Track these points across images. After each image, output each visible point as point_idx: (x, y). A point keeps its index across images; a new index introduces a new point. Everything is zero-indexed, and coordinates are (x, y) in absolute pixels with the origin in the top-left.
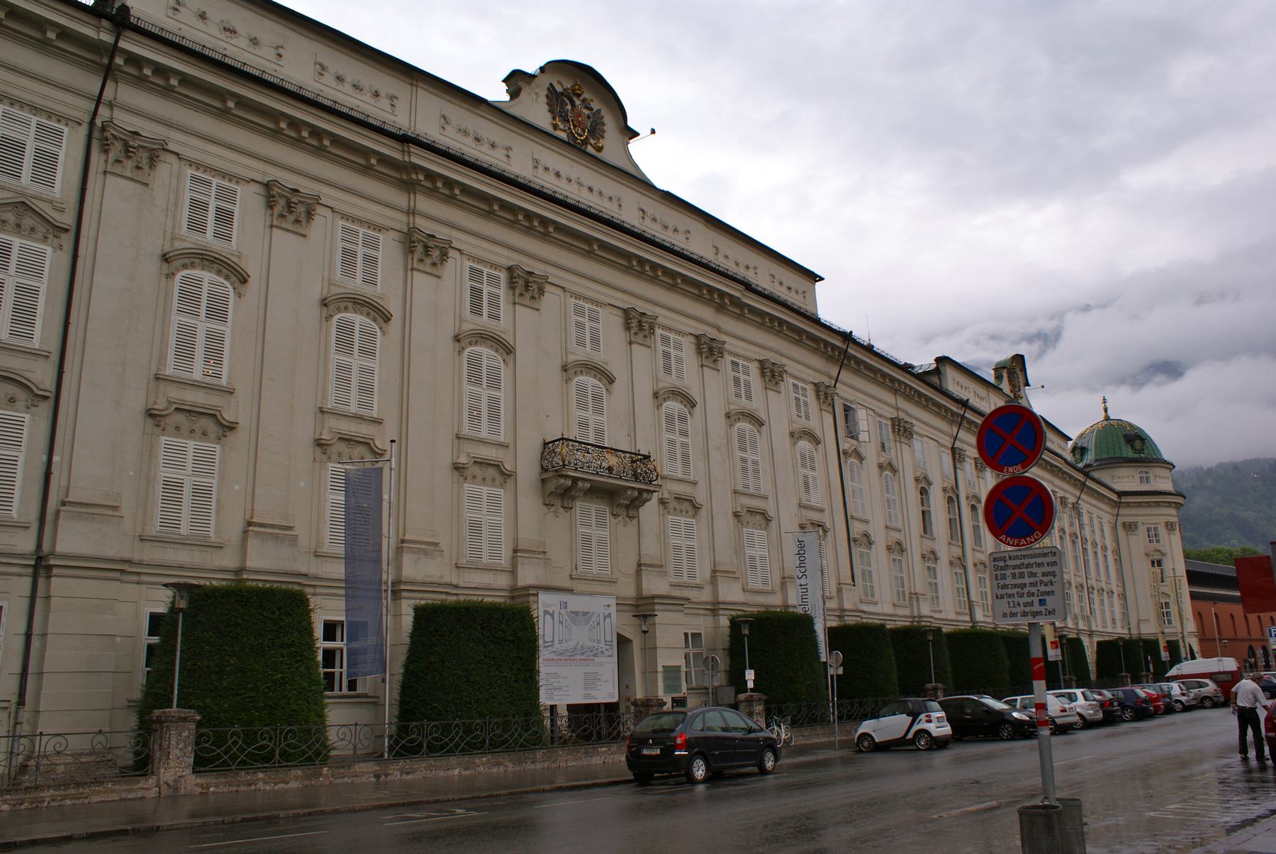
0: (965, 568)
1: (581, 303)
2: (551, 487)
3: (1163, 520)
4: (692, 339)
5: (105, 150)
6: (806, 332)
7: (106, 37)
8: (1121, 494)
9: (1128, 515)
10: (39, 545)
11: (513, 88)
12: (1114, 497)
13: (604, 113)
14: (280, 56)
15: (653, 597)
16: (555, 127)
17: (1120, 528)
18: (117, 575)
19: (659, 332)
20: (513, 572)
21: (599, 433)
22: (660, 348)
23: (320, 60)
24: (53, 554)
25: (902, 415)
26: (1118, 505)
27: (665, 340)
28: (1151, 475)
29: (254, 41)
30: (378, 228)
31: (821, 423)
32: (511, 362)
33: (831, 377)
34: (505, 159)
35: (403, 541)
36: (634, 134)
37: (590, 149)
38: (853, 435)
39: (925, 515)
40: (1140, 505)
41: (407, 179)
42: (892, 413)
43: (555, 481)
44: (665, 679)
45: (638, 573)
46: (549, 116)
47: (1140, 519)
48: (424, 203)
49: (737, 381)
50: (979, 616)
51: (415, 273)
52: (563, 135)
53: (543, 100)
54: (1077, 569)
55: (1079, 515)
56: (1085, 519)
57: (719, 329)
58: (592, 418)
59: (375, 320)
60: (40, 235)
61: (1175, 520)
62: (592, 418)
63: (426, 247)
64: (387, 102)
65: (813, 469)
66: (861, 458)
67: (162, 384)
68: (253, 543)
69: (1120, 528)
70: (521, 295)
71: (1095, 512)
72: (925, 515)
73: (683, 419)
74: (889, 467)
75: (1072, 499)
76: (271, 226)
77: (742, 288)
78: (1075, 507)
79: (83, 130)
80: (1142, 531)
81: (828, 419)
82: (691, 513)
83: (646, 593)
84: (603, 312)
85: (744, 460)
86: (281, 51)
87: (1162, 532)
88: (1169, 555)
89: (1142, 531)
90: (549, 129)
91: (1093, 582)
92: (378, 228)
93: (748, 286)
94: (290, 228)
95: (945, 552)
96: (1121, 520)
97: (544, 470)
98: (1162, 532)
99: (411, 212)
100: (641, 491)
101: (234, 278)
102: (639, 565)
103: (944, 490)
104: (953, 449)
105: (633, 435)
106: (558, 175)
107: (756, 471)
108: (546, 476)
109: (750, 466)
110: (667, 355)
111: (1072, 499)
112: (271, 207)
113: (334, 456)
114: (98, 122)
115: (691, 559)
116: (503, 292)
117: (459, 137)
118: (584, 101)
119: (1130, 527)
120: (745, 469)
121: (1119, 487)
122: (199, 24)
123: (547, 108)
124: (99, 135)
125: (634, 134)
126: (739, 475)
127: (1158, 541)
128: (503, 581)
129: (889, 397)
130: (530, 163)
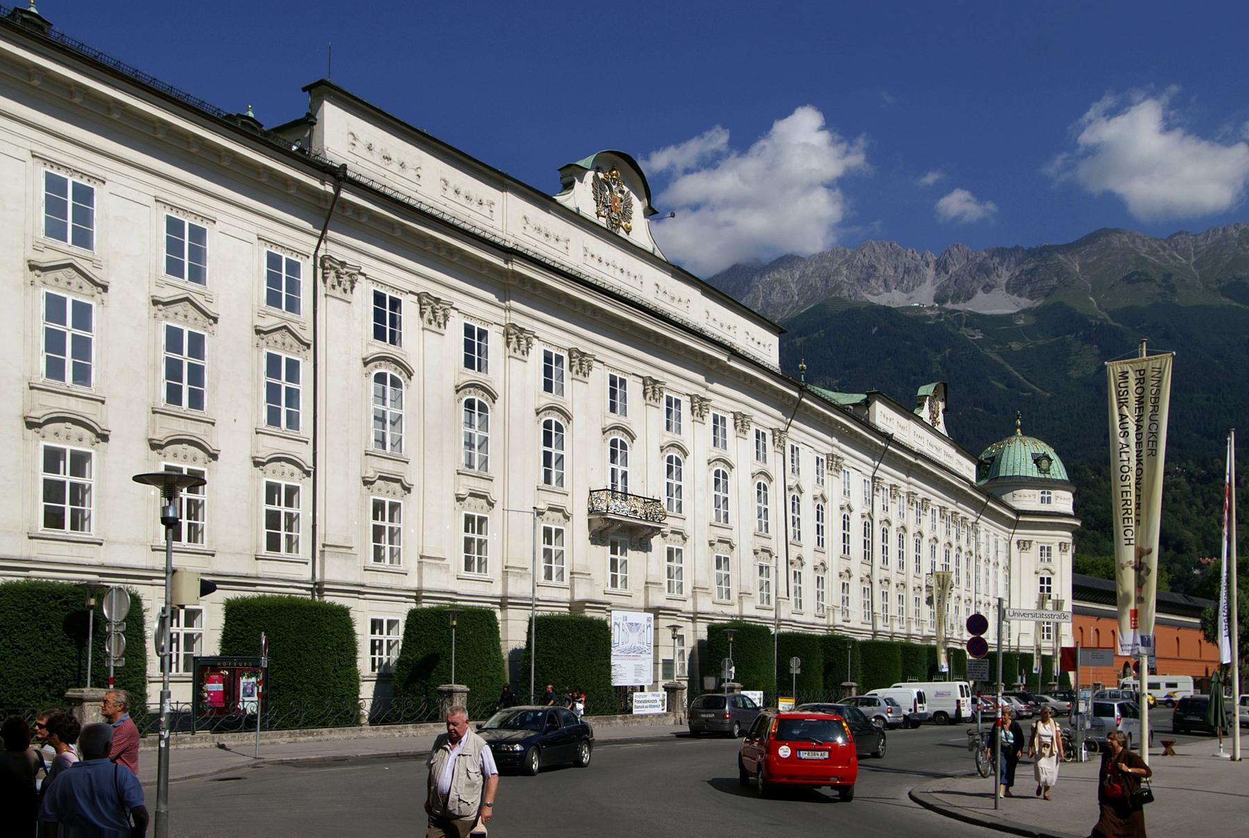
3: (1057, 540)
7: (329, 189)
8: (1019, 513)
10: (314, 575)
19: (666, 393)
31: (774, 463)
34: (564, 250)
37: (622, 233)
38: (796, 471)
39: (846, 538)
45: (646, 588)
52: (602, 222)
54: (969, 584)
55: (977, 532)
56: (982, 535)
60: (295, 350)
61: (1070, 541)
69: (1014, 546)
71: (993, 530)
72: (846, 538)
80: (1035, 549)
88: (1058, 574)
89: (1035, 549)
91: (981, 597)
98: (1055, 550)
104: (874, 478)
106: (600, 261)
111: (972, 519)
117: (535, 234)
119: (1024, 545)
127: (1049, 560)
130: (582, 252)
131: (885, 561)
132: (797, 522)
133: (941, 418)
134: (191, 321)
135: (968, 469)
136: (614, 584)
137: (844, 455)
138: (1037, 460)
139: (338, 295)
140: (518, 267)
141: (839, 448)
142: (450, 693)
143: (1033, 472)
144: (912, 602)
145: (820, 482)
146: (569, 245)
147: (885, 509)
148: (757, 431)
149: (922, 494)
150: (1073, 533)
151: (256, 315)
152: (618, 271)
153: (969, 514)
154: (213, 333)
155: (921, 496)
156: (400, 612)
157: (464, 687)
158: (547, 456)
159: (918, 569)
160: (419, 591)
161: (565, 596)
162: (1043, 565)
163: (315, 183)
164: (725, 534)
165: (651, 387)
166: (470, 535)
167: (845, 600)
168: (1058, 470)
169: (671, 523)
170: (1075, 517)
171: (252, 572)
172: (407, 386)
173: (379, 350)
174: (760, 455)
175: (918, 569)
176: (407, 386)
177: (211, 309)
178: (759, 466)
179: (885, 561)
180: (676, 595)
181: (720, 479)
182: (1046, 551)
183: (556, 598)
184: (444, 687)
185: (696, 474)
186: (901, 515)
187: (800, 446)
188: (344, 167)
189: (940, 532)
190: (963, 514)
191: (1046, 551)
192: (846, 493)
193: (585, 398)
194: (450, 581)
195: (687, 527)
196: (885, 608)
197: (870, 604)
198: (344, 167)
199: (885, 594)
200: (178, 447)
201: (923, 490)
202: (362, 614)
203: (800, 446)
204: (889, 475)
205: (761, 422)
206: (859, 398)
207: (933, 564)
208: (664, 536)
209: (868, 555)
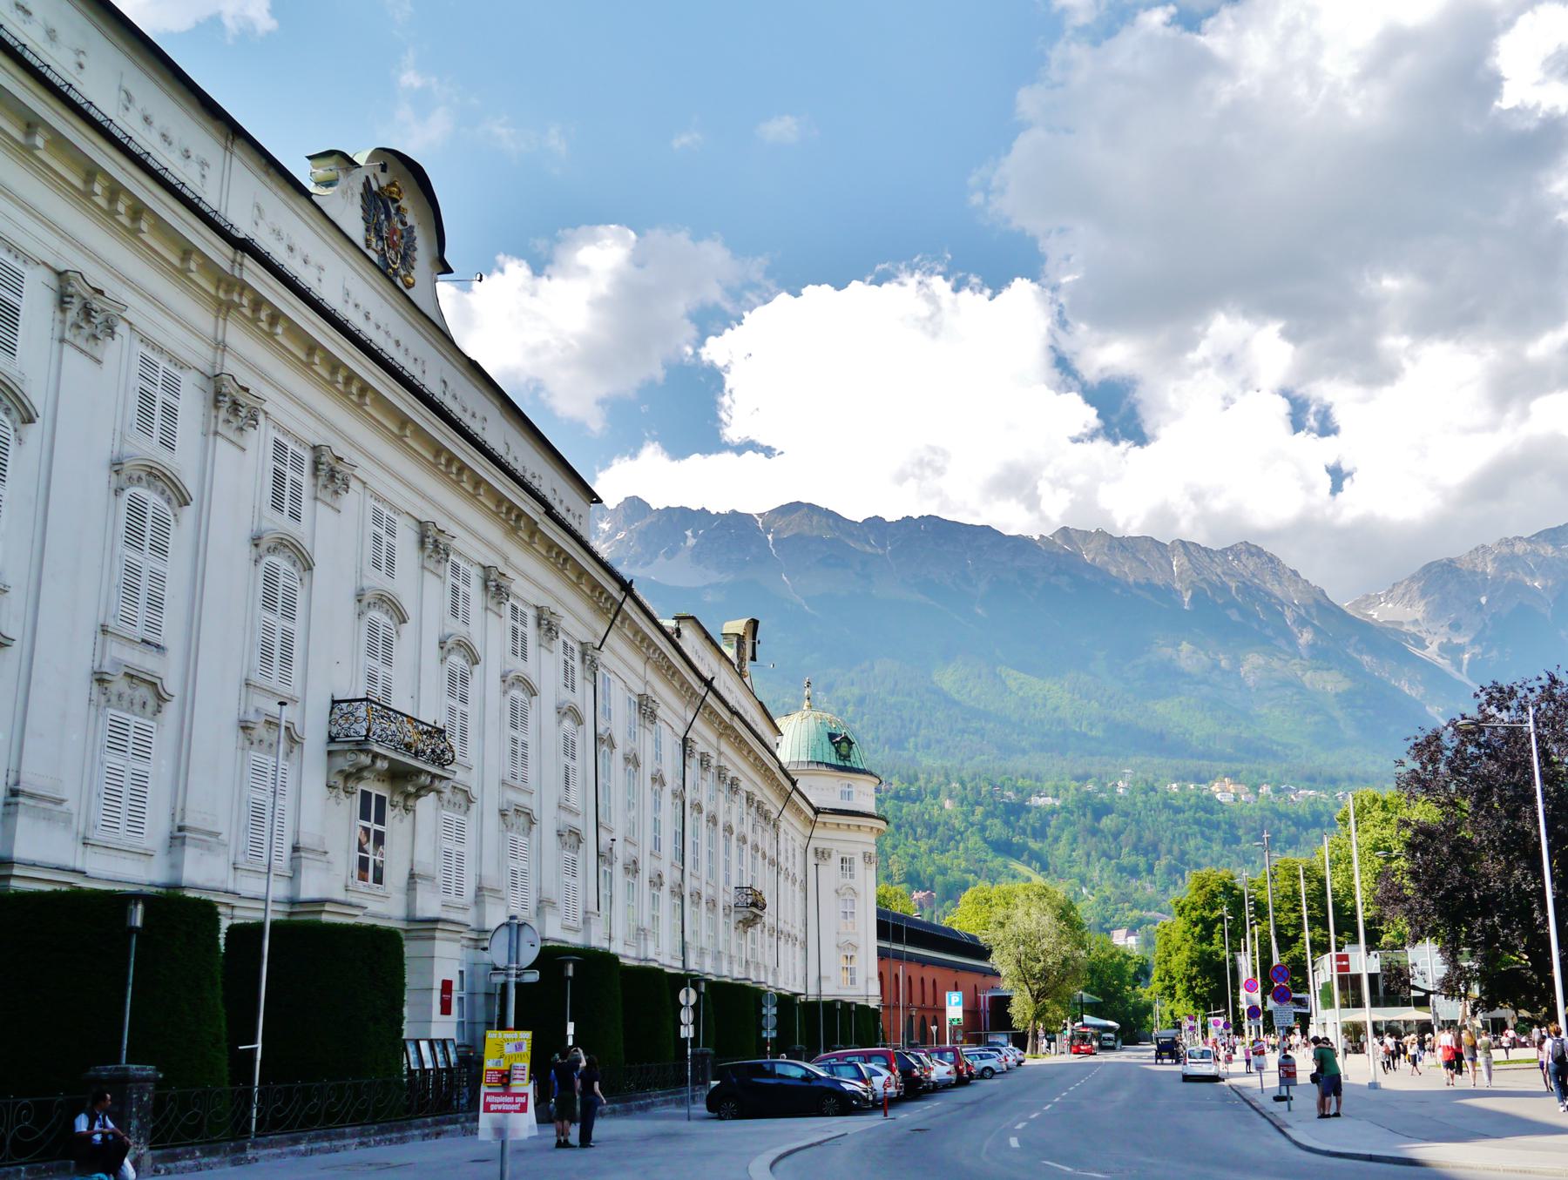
1: (379, 506)
2: (343, 763)
8: (817, 811)
12: (810, 813)
13: (418, 233)
14: (81, 66)
16: (367, 241)
19: (452, 557)
20: (294, 876)
21: (387, 691)
22: (450, 580)
23: (127, 85)
25: (649, 693)
26: (813, 823)
27: (455, 568)
29: (51, 34)
32: (306, 581)
35: (181, 829)
42: (639, 688)
48: (238, 337)
49: (515, 631)
51: (219, 439)
52: (374, 257)
53: (358, 200)
56: (782, 836)
58: (382, 670)
59: (169, 501)
61: (873, 850)
62: (382, 670)
64: (197, 168)
65: (573, 758)
66: (613, 746)
70: (325, 487)
71: (791, 832)
73: (464, 680)
74: (632, 760)
75: (774, 815)
76: (62, 340)
77: (541, 510)
78: (776, 826)
80: (835, 861)
82: (464, 808)
83: (420, 914)
85: (514, 741)
86: (82, 59)
87: (859, 862)
89: (835, 861)
90: (361, 243)
93: (549, 511)
94: (84, 346)
97: (332, 739)
98: (859, 862)
101: (15, 414)
104: (685, 740)
105: (416, 698)
106: (367, 317)
107: (525, 756)
108: (334, 747)
109: (520, 750)
110: (455, 590)
112: (63, 310)
113: (114, 699)
115: (460, 870)
116: (306, 480)
118: (398, 208)
120: (514, 752)
123: (360, 212)
126: (508, 761)
127: (852, 876)
128: (280, 889)
129: (637, 662)
131: (696, 862)
145: (632, 734)
147: (696, 788)
153: (772, 802)
155: (730, 774)
157: (149, 1070)
165: (432, 542)
167: (655, 918)
172: (20, 441)
176: (20, 441)
179: (696, 862)
180: (453, 898)
184: (106, 1071)
187: (612, 677)
189: (747, 829)
192: (658, 757)
204: (705, 737)
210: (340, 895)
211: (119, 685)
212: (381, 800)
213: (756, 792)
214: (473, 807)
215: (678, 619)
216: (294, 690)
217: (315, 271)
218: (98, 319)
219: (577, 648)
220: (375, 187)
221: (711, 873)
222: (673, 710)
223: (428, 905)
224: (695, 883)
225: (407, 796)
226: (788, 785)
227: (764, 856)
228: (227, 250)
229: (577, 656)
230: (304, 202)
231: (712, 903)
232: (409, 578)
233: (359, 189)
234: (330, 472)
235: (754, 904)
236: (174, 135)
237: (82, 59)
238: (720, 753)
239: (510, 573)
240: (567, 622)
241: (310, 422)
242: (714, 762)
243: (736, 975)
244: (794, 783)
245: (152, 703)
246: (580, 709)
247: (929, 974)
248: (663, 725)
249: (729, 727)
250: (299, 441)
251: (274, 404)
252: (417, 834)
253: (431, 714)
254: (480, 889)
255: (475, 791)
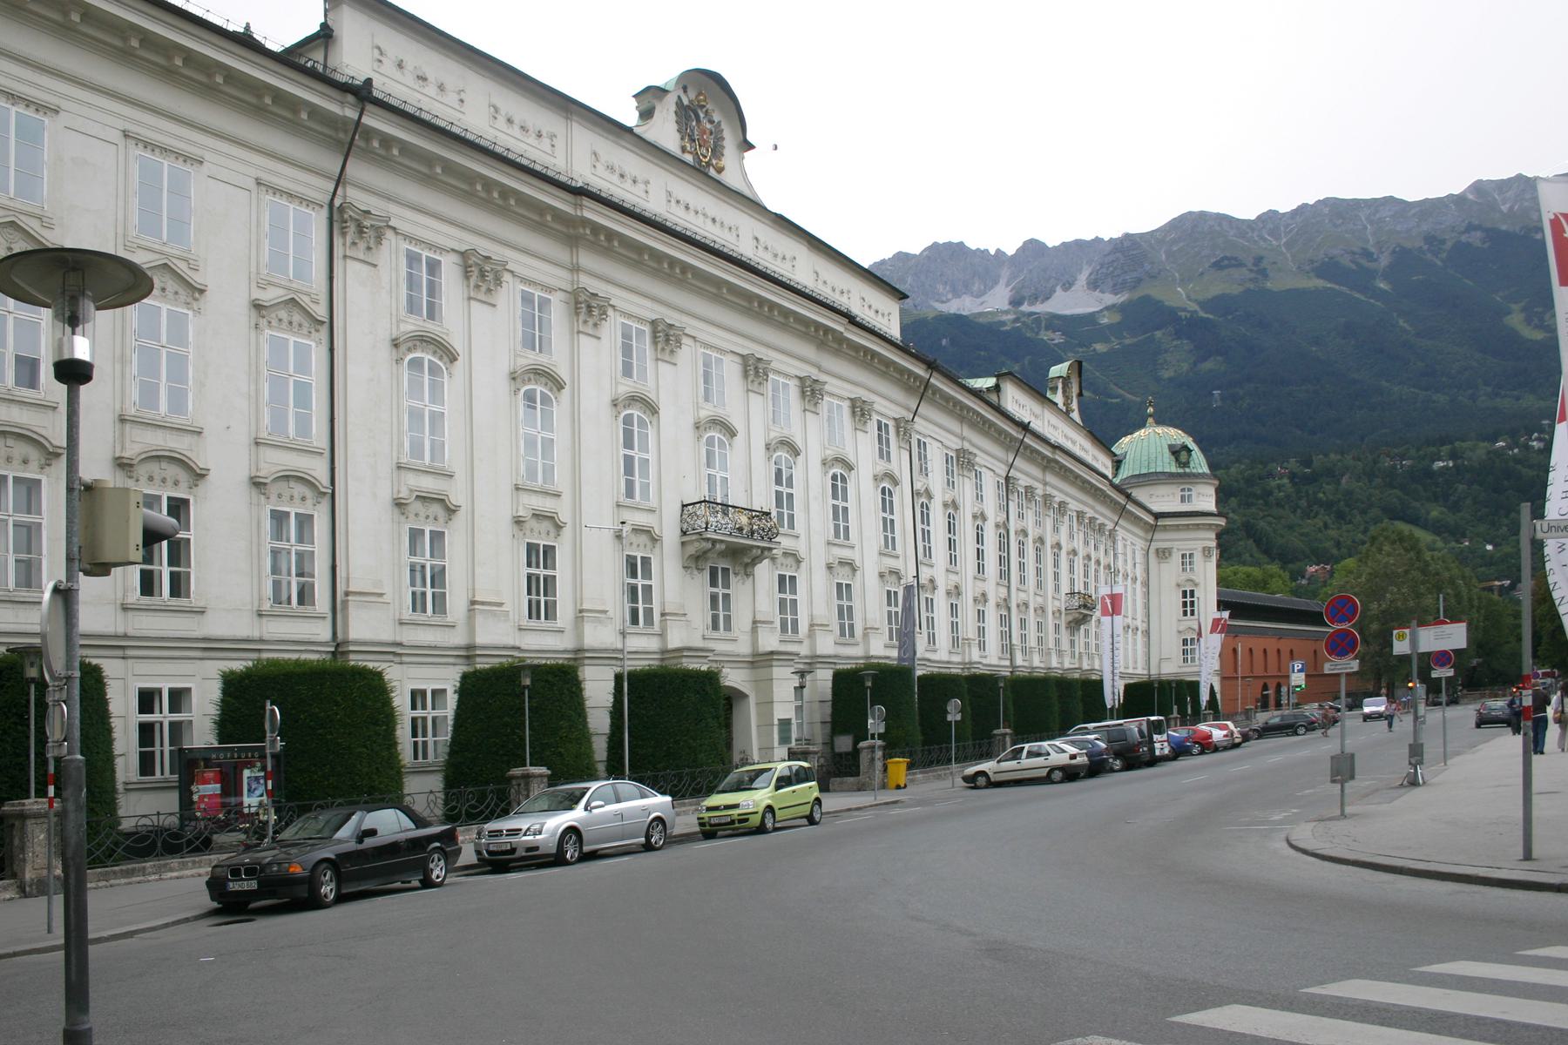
0: (1009, 609)
2: (691, 550)
3: (1199, 545)
4: (796, 382)
5: (344, 234)
6: (894, 363)
7: (351, 114)
8: (1158, 516)
9: (1162, 540)
11: (645, 106)
12: (1151, 520)
15: (772, 653)
16: (684, 150)
17: (1152, 551)
18: (391, 657)
20: (662, 635)
23: (495, 101)
24: (346, 642)
25: (967, 446)
28: (1194, 493)
29: (441, 88)
30: (549, 289)
31: (899, 463)
33: (908, 410)
34: (643, 195)
36: (751, 147)
37: (712, 172)
38: (924, 471)
40: (1177, 528)
41: (573, 233)
42: (955, 443)
43: (697, 544)
44: (780, 731)
45: (754, 630)
46: (678, 136)
47: (1176, 545)
48: (587, 259)
50: (1019, 661)
52: (689, 158)
53: (673, 117)
56: (1120, 545)
57: (819, 368)
60: (305, 331)
61: (1214, 544)
63: (589, 307)
67: (403, 472)
68: (479, 620)
72: (980, 554)
75: (1110, 526)
77: (845, 321)
78: (1112, 534)
79: (324, 213)
80: (1176, 558)
81: (906, 455)
84: (727, 359)
86: (463, 96)
89: (1176, 558)
92: (549, 289)
94: (483, 298)
95: (994, 593)
96: (1154, 545)
97: (684, 533)
98: (1198, 557)
99: (575, 269)
100: (763, 549)
102: (755, 622)
103: (997, 526)
104: (1007, 478)
105: (749, 491)
106: (687, 208)
108: (686, 539)
111: (1110, 526)
114: (337, 203)
117: (607, 175)
119: (1163, 554)
121: (1157, 507)
122: (417, 85)
123: (675, 127)
124: (338, 218)
125: (751, 147)
129: (954, 425)
130: (664, 196)
131: (1022, 580)
132: (926, 535)
133: (1075, 405)
134: (171, 296)
135: (1103, 463)
136: (715, 627)
137: (975, 451)
138: (1178, 452)
139: (361, 256)
140: (593, 213)
141: (970, 442)
142: (527, 777)
143: (1173, 469)
144: (1051, 628)
145: (950, 484)
146: (650, 188)
147: (1021, 516)
148: (879, 423)
149: (1059, 497)
150: (1218, 537)
151: (254, 285)
152: (709, 222)
153: (1105, 517)
154: (198, 312)
155: (1057, 499)
156: (448, 679)
158: (629, 461)
159: (1057, 588)
160: (470, 647)
161: (653, 644)
162: (1184, 576)
163: (334, 108)
164: (845, 553)
165: (754, 370)
166: (533, 571)
167: (981, 631)
168: (1199, 463)
169: (785, 542)
170: (1219, 515)
171: (256, 634)
172: (450, 374)
173: (413, 328)
174: (884, 454)
175: (1057, 588)
176: (450, 374)
177: (197, 278)
178: (882, 466)
179: (1022, 580)
181: (838, 487)
182: (1187, 559)
183: (643, 648)
185: (810, 481)
186: (1038, 523)
188: (369, 82)
189: (1078, 543)
190: (1101, 520)
191: (1187, 559)
192: (979, 498)
193: (674, 385)
194: (508, 634)
195: (801, 547)
196: (1023, 638)
197: (1006, 635)
198: (369, 82)
199: (1023, 622)
200: (154, 467)
201: (1061, 490)
202: (402, 681)
203: (927, 440)
204: (1027, 473)
205: (883, 410)
206: (990, 382)
207: (1072, 581)
208: (773, 559)
209: (1005, 574)
210: (699, 644)
211: (533, 523)
212: (726, 570)
213: (1086, 509)
214: (803, 565)
215: (998, 377)
216: (653, 503)
217: (642, 186)
218: (490, 277)
219: (891, 424)
220: (686, 102)
221: (1039, 585)
222: (991, 460)
223: (770, 641)
224: (1023, 595)
225: (747, 565)
226: (1121, 500)
227: (1098, 562)
228: (569, 197)
229: (892, 430)
230: (628, 136)
231: (1042, 610)
232: (733, 400)
233: (673, 108)
234: (665, 337)
235: (1085, 606)
236: (529, 125)
237: (463, 96)
238: (1045, 484)
239: (823, 377)
240: (880, 405)
241: (648, 303)
242: (1039, 492)
243: (1067, 665)
244: (1128, 497)
245: (552, 530)
246: (897, 473)
247: (1286, 645)
248: (984, 470)
249: (1050, 460)
250: (640, 320)
251: (618, 297)
252: (756, 594)
253: (763, 499)
254: (812, 625)
255: (803, 553)
